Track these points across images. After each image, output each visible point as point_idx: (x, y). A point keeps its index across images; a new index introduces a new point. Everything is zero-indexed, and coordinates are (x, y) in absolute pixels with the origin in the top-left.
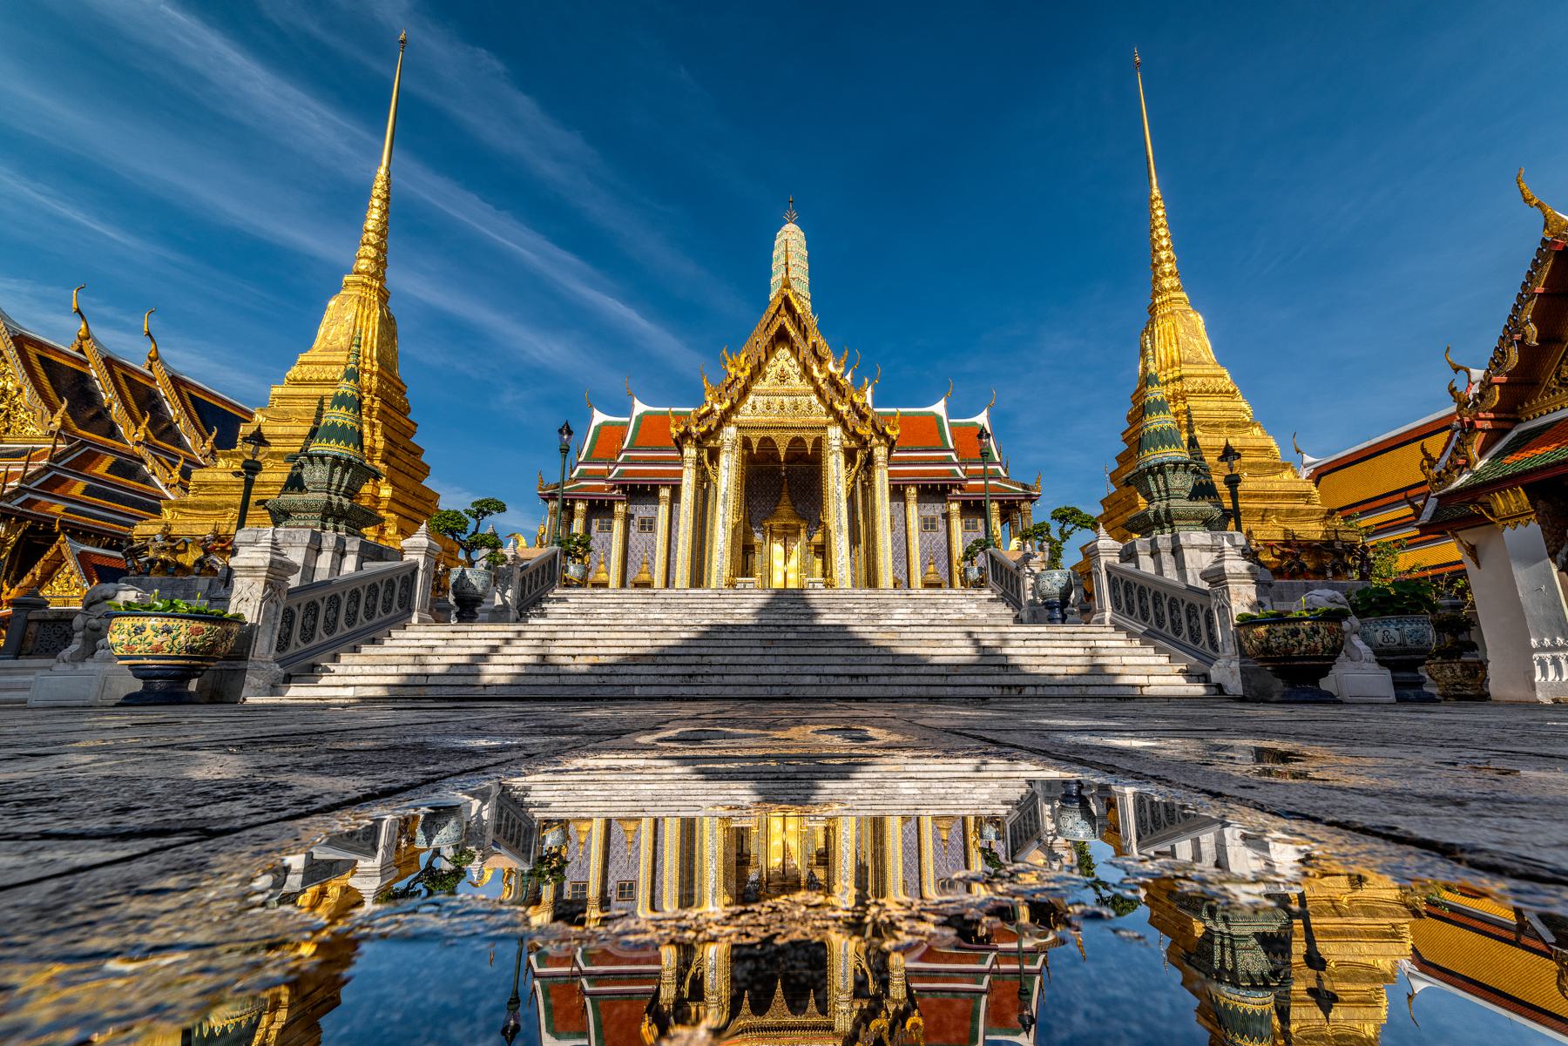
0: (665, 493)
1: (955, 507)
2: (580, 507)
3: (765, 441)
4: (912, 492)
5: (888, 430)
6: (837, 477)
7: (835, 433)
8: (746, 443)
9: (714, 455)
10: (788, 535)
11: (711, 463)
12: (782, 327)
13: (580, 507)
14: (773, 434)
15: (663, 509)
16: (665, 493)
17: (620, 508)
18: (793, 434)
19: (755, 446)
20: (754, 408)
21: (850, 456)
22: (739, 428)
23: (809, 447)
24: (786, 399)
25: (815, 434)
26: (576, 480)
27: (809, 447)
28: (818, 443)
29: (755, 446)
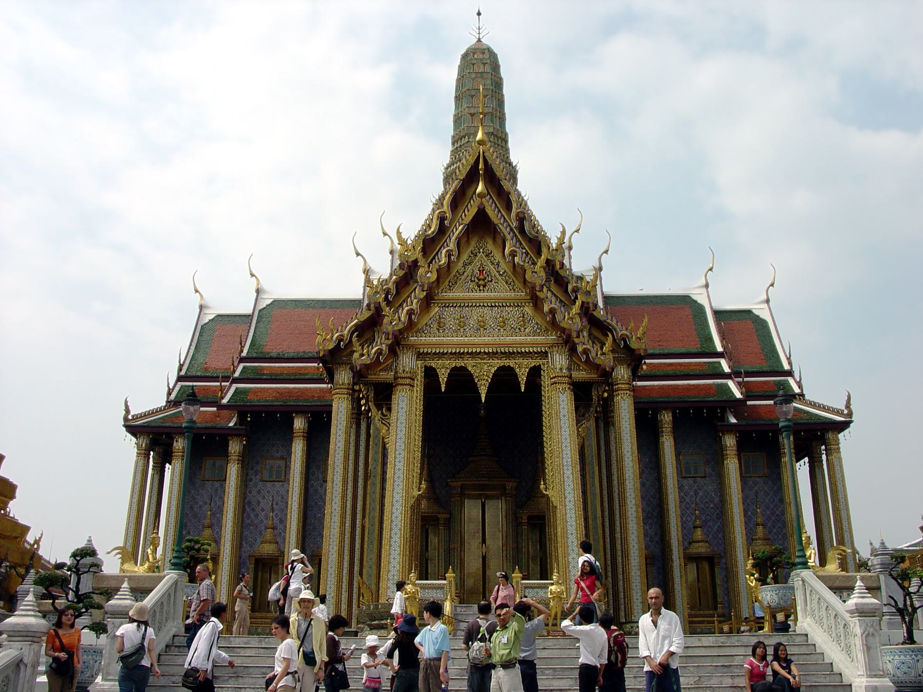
1: (730, 441)
4: (666, 418)
7: (559, 360)
8: (430, 374)
9: (384, 395)
11: (379, 408)
12: (481, 214)
13: (179, 444)
15: (298, 448)
16: (299, 424)
17: (235, 447)
18: (498, 363)
19: (443, 378)
20: (441, 326)
21: (582, 394)
22: (420, 356)
24: (486, 310)
25: (533, 363)
28: (535, 372)
29: (443, 378)
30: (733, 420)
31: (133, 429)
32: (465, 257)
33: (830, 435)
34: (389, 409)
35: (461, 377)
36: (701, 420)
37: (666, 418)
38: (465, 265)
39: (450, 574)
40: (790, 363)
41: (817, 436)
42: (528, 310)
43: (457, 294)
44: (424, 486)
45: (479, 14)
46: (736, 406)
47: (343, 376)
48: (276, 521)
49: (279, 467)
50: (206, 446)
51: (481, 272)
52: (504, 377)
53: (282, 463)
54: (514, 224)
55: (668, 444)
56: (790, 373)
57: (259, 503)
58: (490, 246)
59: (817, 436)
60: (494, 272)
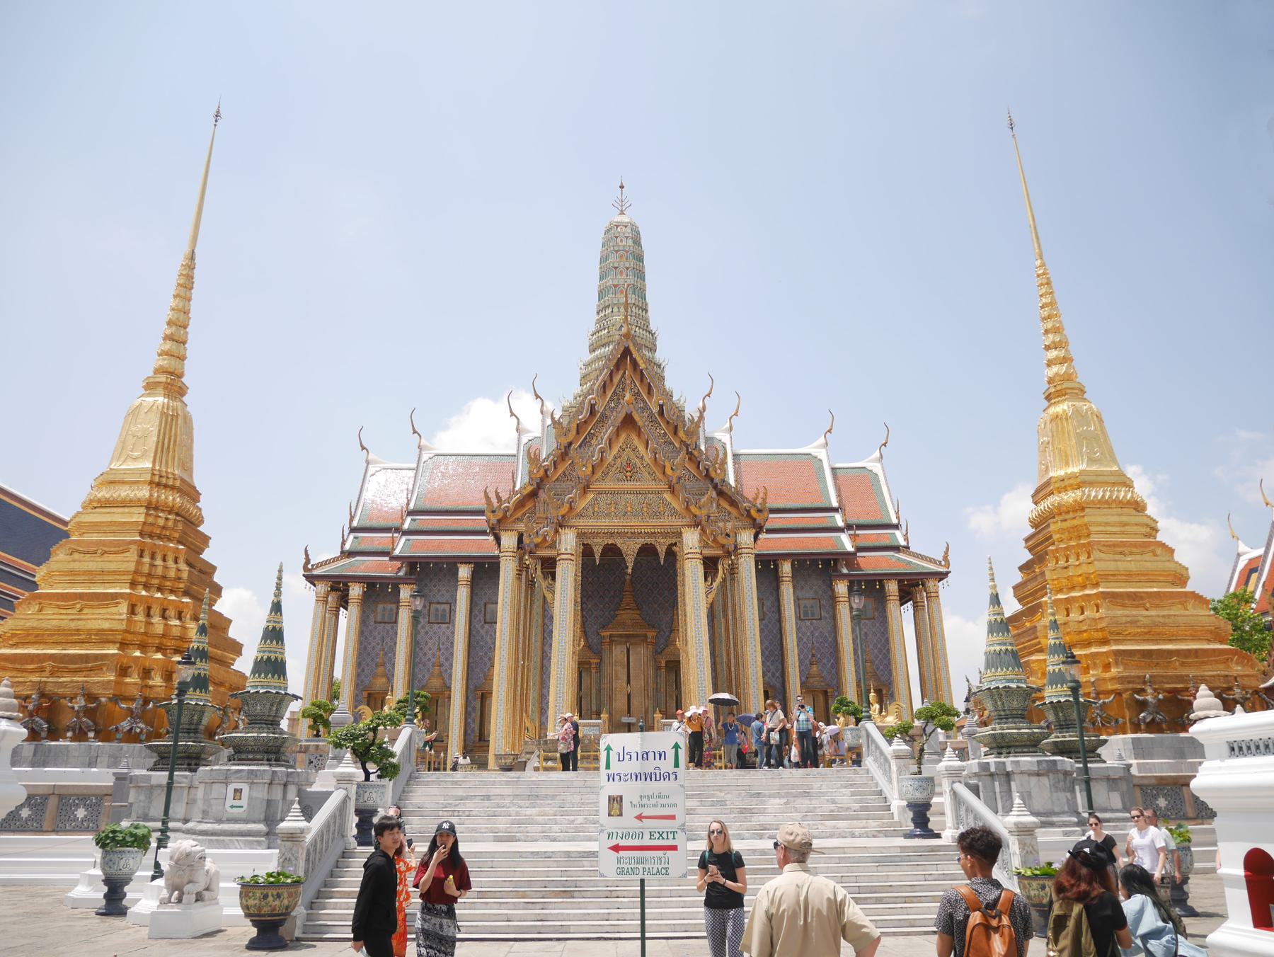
0: (464, 572)
1: (841, 588)
2: (356, 591)
3: (612, 551)
4: (786, 568)
5: (753, 512)
6: (695, 592)
8: (587, 552)
9: (549, 566)
10: (629, 639)
11: (545, 578)
14: (619, 542)
15: (463, 594)
16: (464, 572)
18: (642, 541)
19: (598, 551)
21: (710, 565)
23: (662, 556)
26: (351, 554)
27: (662, 556)
29: (598, 551)
30: (845, 571)
31: (311, 579)
32: (615, 451)
33: (931, 584)
34: (554, 578)
35: (612, 551)
36: (818, 568)
37: (786, 568)
38: (615, 458)
39: (604, 716)
40: (898, 518)
41: (914, 586)
42: (667, 496)
43: (608, 484)
44: (582, 643)
45: (622, 187)
46: (849, 558)
47: (509, 540)
48: (442, 659)
49: (444, 610)
50: (378, 591)
51: (628, 465)
52: (648, 551)
53: (447, 607)
54: (655, 410)
55: (787, 591)
56: (896, 527)
57: (426, 643)
58: (636, 441)
59: (914, 586)
60: (639, 464)
